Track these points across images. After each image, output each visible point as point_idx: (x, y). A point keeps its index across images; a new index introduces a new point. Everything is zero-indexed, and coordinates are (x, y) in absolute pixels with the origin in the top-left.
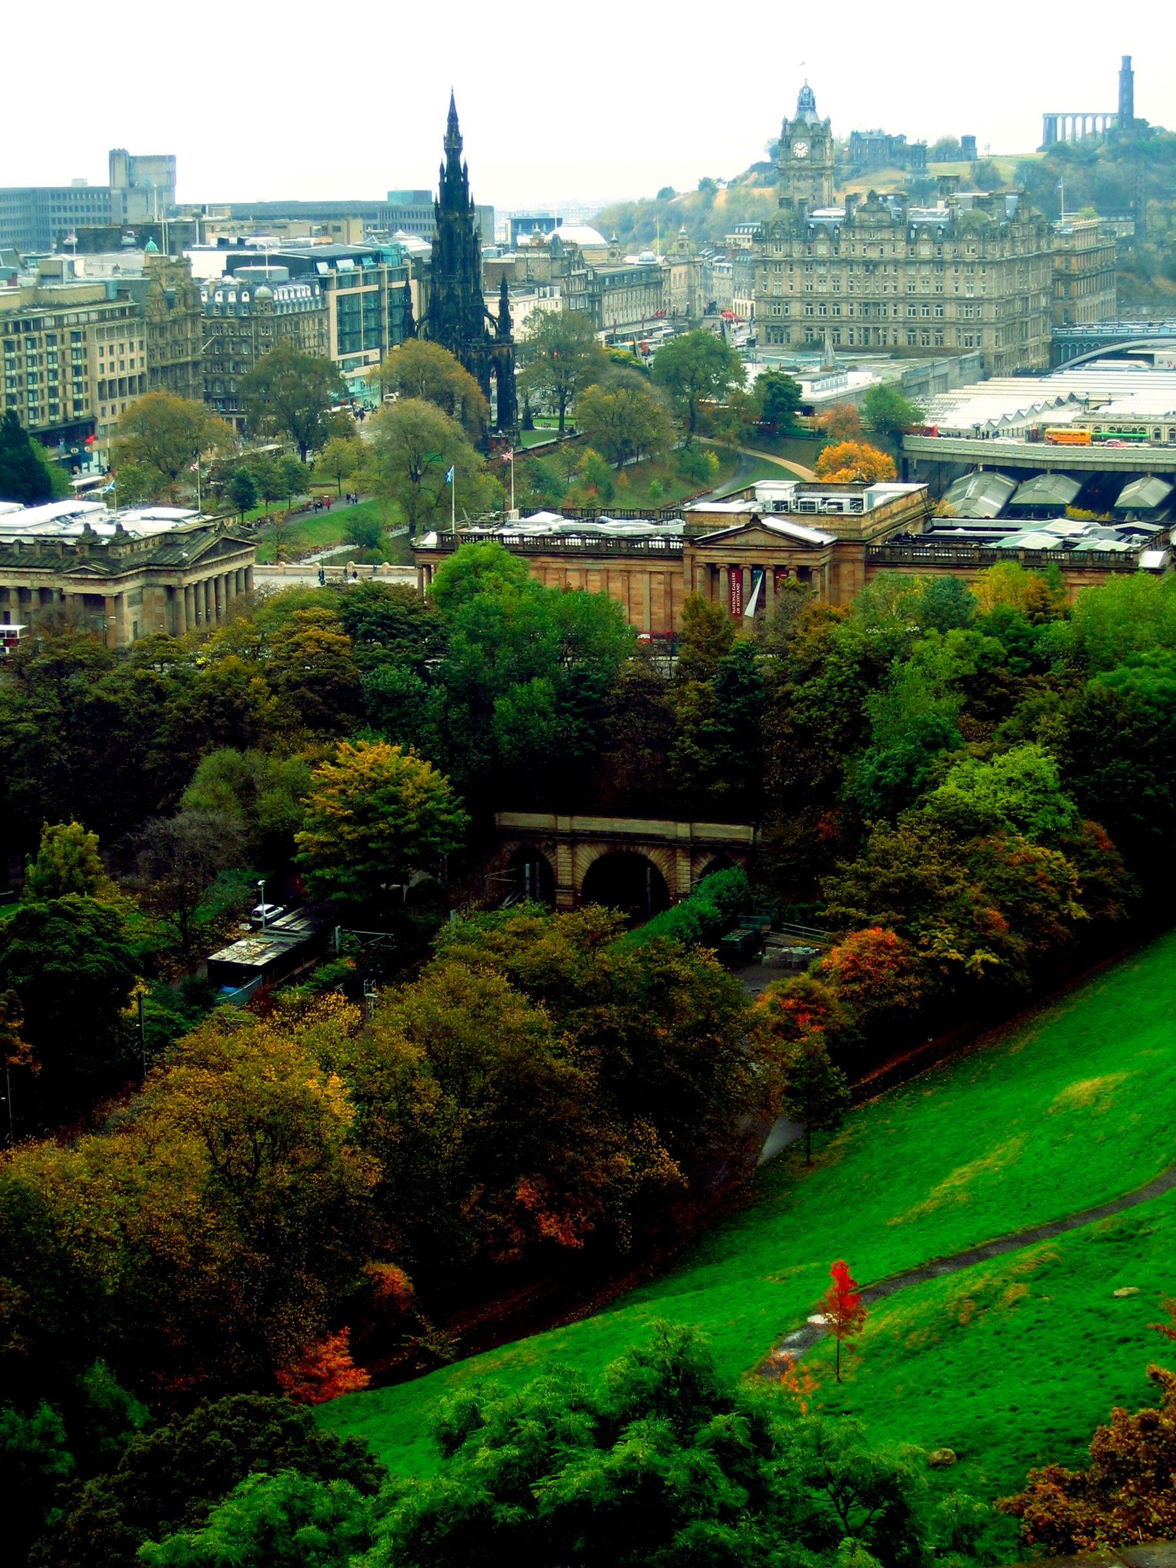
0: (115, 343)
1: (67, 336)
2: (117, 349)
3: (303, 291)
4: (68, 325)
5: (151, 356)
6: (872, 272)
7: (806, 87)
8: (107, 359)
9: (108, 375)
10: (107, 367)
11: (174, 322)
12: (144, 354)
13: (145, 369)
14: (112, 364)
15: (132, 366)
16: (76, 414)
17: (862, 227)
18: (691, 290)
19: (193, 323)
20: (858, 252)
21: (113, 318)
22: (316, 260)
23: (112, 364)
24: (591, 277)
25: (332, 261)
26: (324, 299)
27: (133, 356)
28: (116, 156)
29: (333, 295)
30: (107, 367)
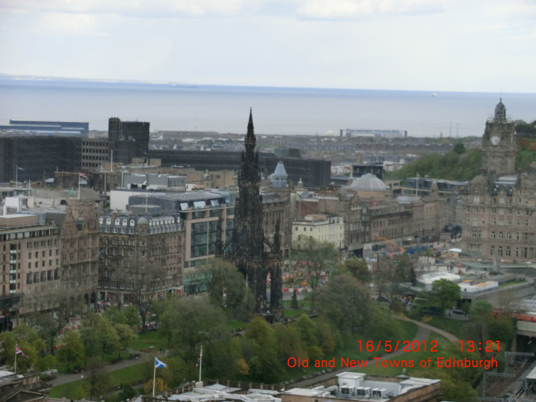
0: (40, 250)
1: (8, 247)
2: (40, 255)
3: (169, 220)
4: (9, 240)
5: (64, 258)
6: (531, 215)
7: (501, 103)
8: (33, 260)
9: (33, 269)
10: (33, 265)
11: (81, 238)
12: (59, 257)
13: (59, 266)
14: (37, 264)
15: (50, 264)
16: (11, 292)
17: (525, 188)
18: (438, 217)
19: (93, 239)
20: (523, 203)
21: (41, 235)
22: (179, 202)
23: (37, 264)
24: (365, 211)
25: (191, 203)
26: (183, 225)
27: (51, 258)
28: (114, 123)
29: (189, 223)
30: (33, 265)
